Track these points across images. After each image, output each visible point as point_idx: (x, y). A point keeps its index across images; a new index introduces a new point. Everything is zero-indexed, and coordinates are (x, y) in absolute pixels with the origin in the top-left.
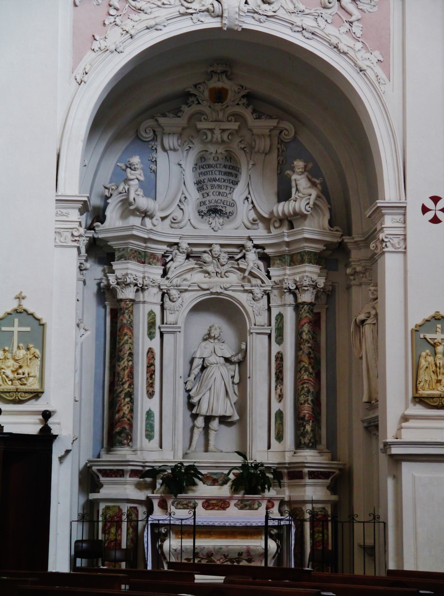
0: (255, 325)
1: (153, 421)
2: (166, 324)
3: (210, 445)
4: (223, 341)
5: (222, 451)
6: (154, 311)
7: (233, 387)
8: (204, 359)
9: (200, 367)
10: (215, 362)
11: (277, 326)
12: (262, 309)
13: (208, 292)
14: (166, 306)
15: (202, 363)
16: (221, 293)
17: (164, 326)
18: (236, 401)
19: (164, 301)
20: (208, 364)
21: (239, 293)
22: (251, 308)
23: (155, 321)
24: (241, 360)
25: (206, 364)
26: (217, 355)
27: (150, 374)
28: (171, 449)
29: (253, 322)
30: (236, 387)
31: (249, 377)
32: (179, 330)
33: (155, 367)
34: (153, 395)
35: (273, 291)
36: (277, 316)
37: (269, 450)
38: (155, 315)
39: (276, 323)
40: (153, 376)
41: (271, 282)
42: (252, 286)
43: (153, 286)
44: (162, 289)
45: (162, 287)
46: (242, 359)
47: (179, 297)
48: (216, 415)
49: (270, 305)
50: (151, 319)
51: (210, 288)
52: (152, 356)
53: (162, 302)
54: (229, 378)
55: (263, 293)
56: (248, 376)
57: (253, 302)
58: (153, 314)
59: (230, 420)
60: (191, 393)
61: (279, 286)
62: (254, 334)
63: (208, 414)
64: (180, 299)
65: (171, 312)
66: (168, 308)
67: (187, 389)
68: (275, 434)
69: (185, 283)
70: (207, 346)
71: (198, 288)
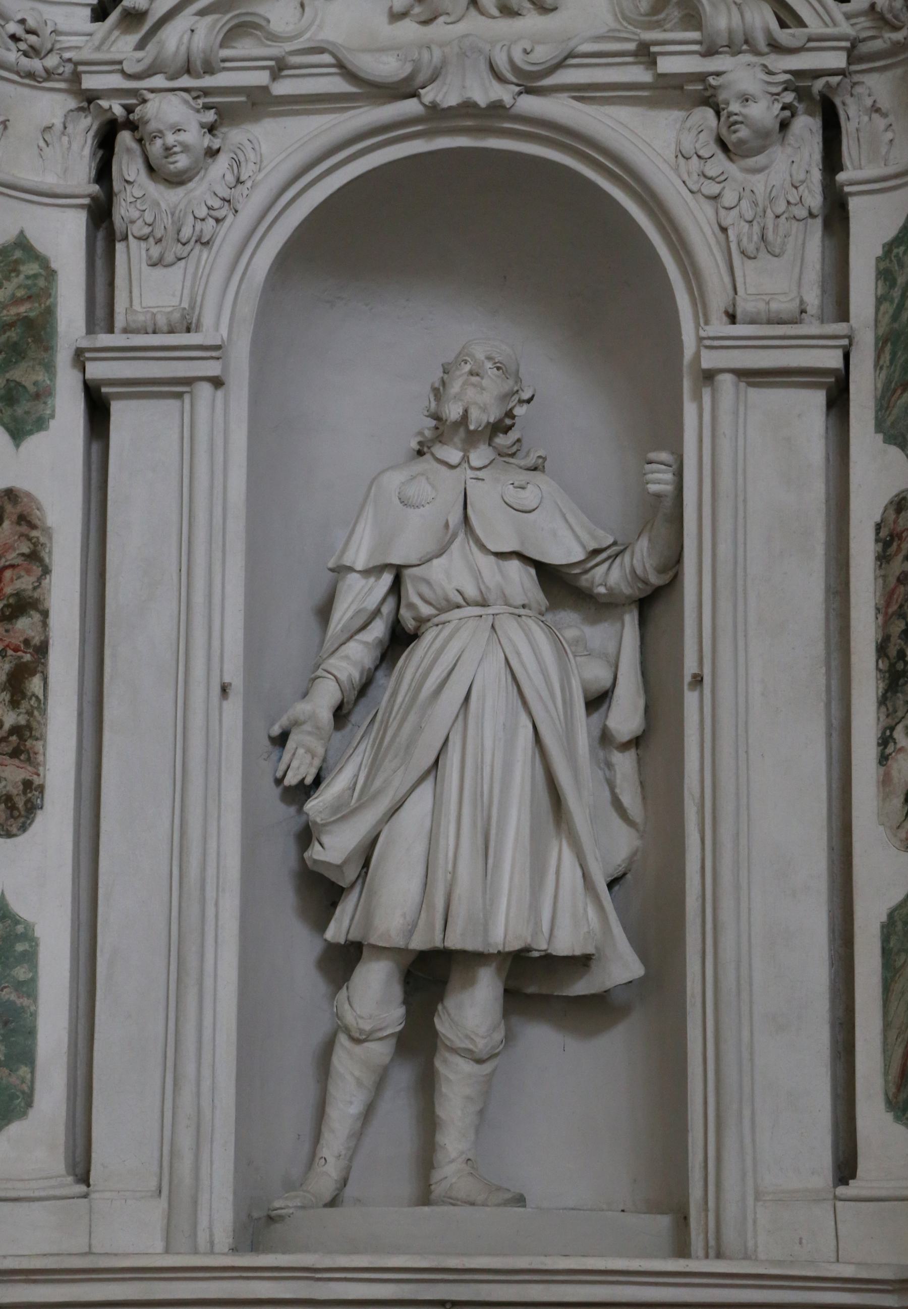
0: (732, 318)
1: (29, 988)
2: (125, 331)
3: (440, 1156)
4: (531, 461)
5: (520, 1200)
6: (40, 244)
7: (609, 765)
8: (399, 573)
9: (378, 630)
10: (471, 592)
11: (886, 320)
12: (781, 207)
13: (410, 107)
14: (123, 211)
15: (388, 609)
16: (497, 108)
17: (104, 340)
18: (631, 860)
19: (117, 185)
20: (426, 610)
21: (624, 113)
22: (708, 208)
23: (49, 313)
24: (655, 580)
25: (411, 606)
26: (482, 547)
27: (7, 667)
28: (153, 1184)
29: (718, 301)
30: (624, 762)
31: (698, 680)
32: (212, 369)
33: (45, 625)
34: (32, 808)
35: (856, 78)
36: (889, 248)
37: (842, 1190)
38: (51, 274)
39: (880, 301)
40: (35, 684)
41: (848, 17)
42: (710, 52)
43: (31, 75)
44: (90, 98)
45: (90, 82)
46: (661, 570)
47: (212, 153)
48: (471, 945)
49: (841, 177)
50: (16, 301)
51: (421, 78)
52: (25, 548)
53: (95, 188)
54: (568, 703)
55: (789, 97)
56: (690, 667)
57: (719, 164)
58: (32, 268)
59: (581, 987)
60: (315, 806)
61: (898, 36)
62: (726, 381)
63: (418, 943)
64: (221, 166)
65: (155, 251)
66: (138, 229)
67: (291, 779)
68: (886, 1073)
69: (245, 47)
70: (420, 490)
71: (337, 85)
